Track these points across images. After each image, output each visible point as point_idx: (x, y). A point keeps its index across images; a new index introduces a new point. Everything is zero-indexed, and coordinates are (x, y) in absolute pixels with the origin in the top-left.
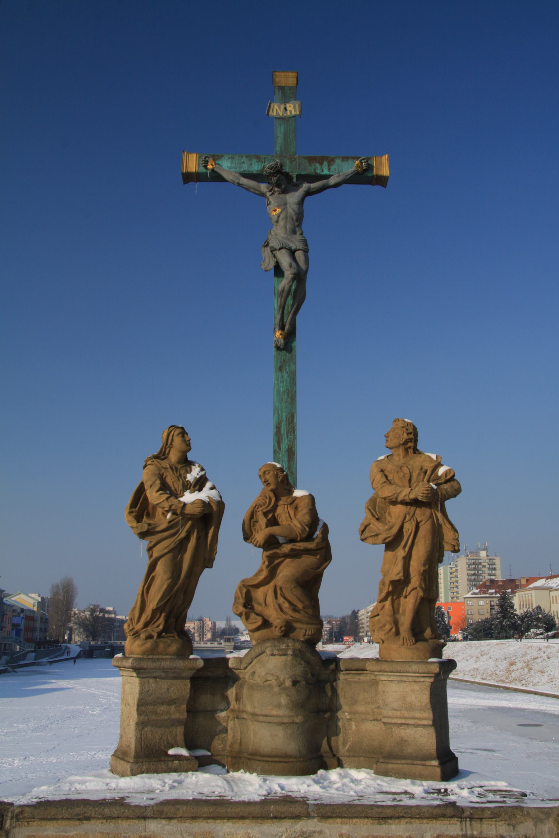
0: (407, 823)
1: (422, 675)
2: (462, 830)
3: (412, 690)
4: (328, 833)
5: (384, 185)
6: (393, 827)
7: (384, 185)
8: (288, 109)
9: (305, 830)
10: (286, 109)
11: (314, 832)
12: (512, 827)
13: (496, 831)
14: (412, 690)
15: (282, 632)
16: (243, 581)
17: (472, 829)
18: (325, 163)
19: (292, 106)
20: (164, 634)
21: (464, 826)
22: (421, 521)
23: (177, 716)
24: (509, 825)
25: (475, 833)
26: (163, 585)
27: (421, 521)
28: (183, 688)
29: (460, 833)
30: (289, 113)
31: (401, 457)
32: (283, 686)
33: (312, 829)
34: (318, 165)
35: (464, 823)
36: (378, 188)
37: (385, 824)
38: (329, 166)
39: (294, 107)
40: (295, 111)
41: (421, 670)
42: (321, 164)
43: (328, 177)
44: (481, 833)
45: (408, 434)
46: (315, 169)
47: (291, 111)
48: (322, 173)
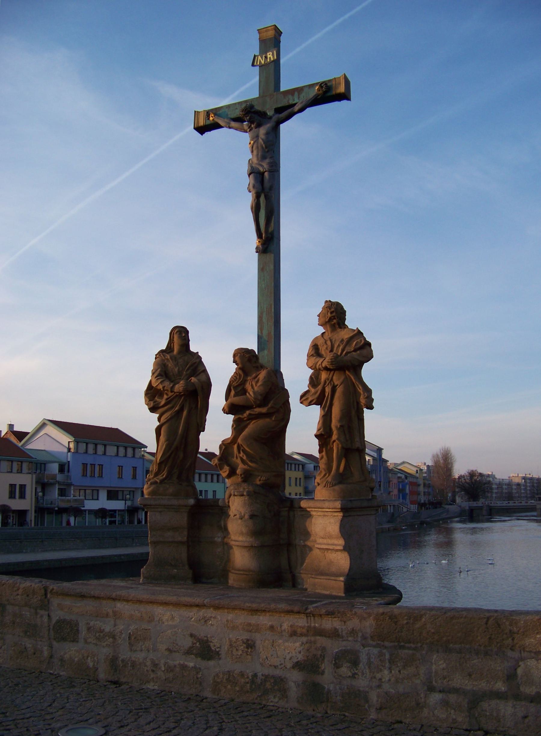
0: (270, 615)
1: (333, 510)
2: (308, 623)
3: (330, 523)
4: (220, 619)
5: (348, 99)
6: (261, 618)
7: (348, 99)
8: (268, 56)
9: (205, 615)
10: (266, 57)
11: (211, 617)
12: (343, 623)
13: (332, 625)
14: (330, 523)
15: (242, 478)
16: (223, 441)
17: (315, 623)
18: (296, 93)
19: (271, 53)
20: (166, 481)
21: (309, 620)
22: (337, 385)
23: (180, 539)
24: (341, 621)
25: (317, 625)
26: (163, 445)
27: (337, 385)
28: (182, 519)
29: (307, 625)
30: (268, 60)
31: (330, 333)
32: (244, 519)
33: (209, 615)
34: (290, 96)
35: (309, 618)
36: (345, 102)
37: (256, 615)
38: (299, 95)
39: (273, 55)
40: (273, 57)
41: (331, 507)
42: (293, 95)
43: (294, 105)
44: (321, 625)
45: (331, 313)
46: (288, 101)
47: (270, 58)
48: (294, 103)
